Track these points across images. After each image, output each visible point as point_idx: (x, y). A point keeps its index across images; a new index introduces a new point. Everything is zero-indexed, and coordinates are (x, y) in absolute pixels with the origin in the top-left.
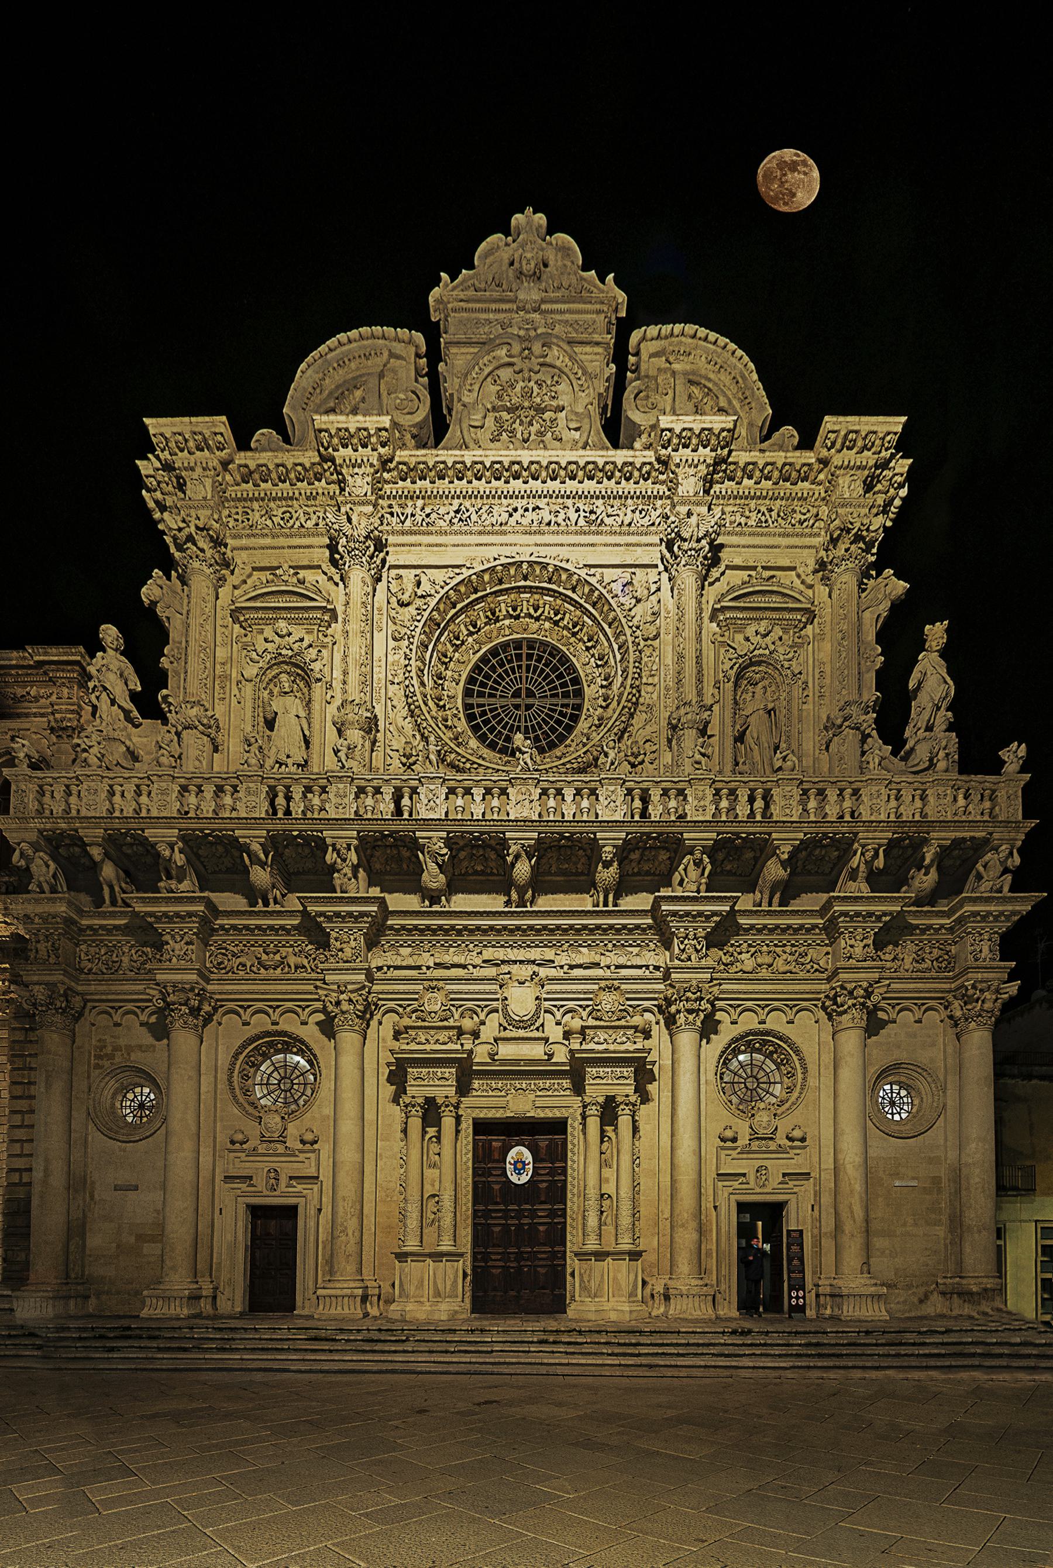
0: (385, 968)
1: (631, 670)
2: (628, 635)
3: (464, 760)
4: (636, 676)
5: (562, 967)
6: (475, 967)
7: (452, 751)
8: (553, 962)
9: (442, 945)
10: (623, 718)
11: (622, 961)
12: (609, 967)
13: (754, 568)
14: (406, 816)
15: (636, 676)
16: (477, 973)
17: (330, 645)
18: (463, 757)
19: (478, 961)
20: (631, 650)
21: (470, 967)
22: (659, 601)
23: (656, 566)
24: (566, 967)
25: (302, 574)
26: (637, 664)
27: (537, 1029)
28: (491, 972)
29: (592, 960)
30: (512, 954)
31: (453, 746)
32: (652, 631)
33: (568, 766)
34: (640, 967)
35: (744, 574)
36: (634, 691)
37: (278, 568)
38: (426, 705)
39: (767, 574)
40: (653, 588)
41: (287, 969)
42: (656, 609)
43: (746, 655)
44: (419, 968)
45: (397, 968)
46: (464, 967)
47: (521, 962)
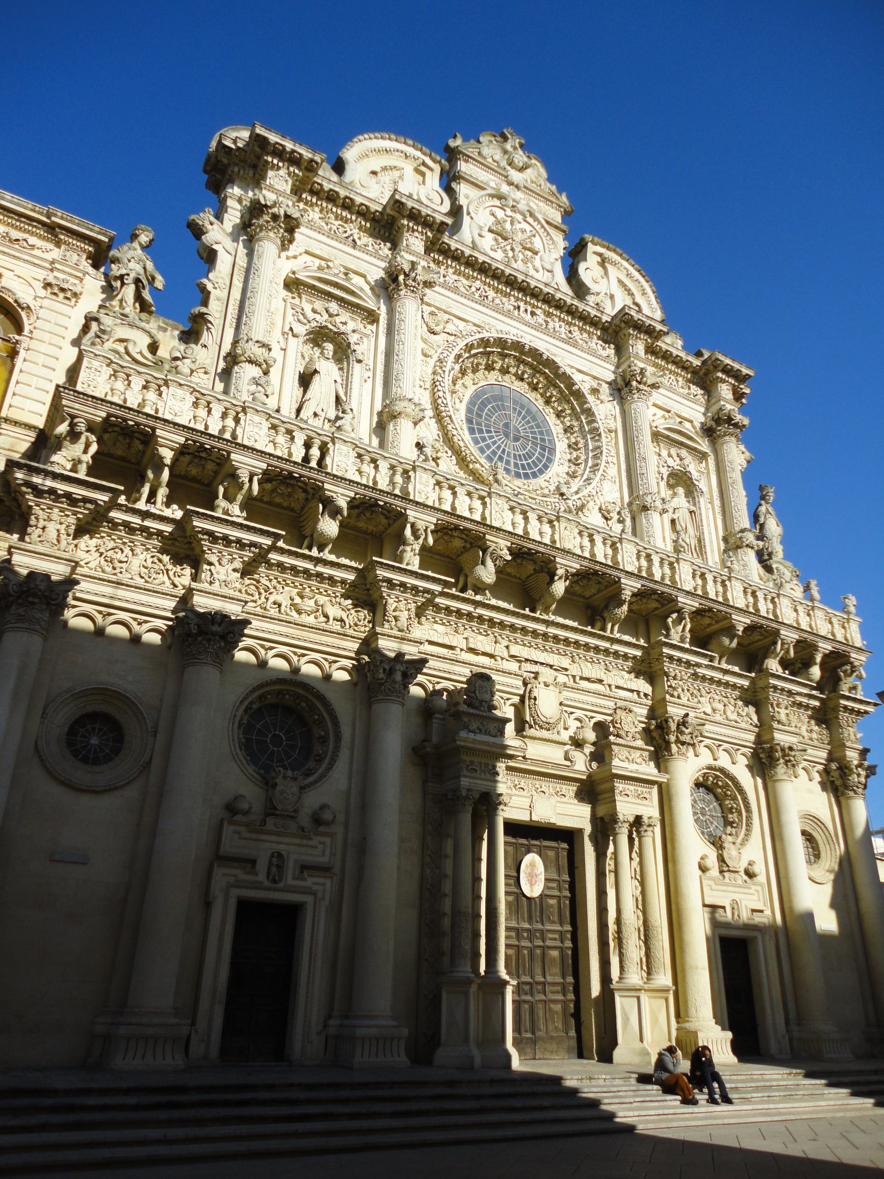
5: (574, 677)
6: (502, 659)
8: (566, 670)
11: (621, 683)
12: (610, 686)
13: (669, 412)
21: (499, 659)
25: (352, 275)
29: (599, 677)
34: (632, 691)
41: (325, 619)
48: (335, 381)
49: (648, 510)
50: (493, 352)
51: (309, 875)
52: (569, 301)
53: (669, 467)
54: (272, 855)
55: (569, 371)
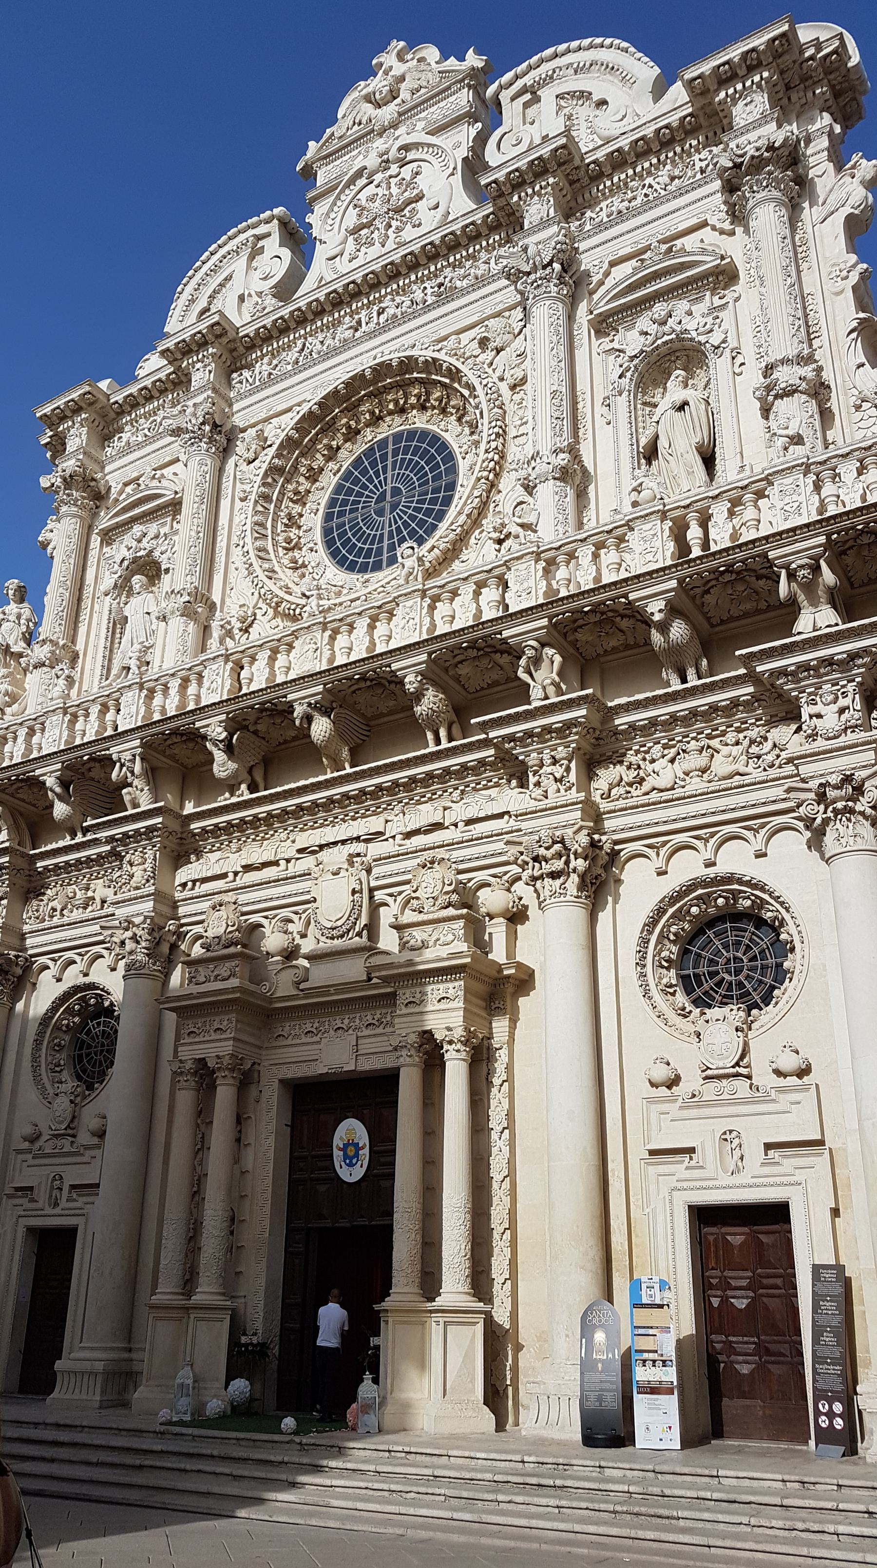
0: (190, 884)
3: (293, 607)
5: (393, 837)
6: (288, 861)
7: (282, 600)
9: (254, 840)
11: (471, 813)
12: (456, 825)
15: (493, 437)
16: (296, 868)
19: (292, 853)
24: (399, 837)
26: (493, 424)
27: (359, 934)
28: (307, 863)
30: (329, 834)
34: (500, 816)
35: (633, 263)
36: (490, 456)
37: (141, 476)
39: (664, 247)
43: (642, 351)
44: (224, 876)
45: (204, 880)
46: (276, 863)
47: (343, 842)
48: (148, 613)
51: (79, 1195)
52: (285, 312)
53: (632, 358)
54: (54, 1179)
55: (429, 354)
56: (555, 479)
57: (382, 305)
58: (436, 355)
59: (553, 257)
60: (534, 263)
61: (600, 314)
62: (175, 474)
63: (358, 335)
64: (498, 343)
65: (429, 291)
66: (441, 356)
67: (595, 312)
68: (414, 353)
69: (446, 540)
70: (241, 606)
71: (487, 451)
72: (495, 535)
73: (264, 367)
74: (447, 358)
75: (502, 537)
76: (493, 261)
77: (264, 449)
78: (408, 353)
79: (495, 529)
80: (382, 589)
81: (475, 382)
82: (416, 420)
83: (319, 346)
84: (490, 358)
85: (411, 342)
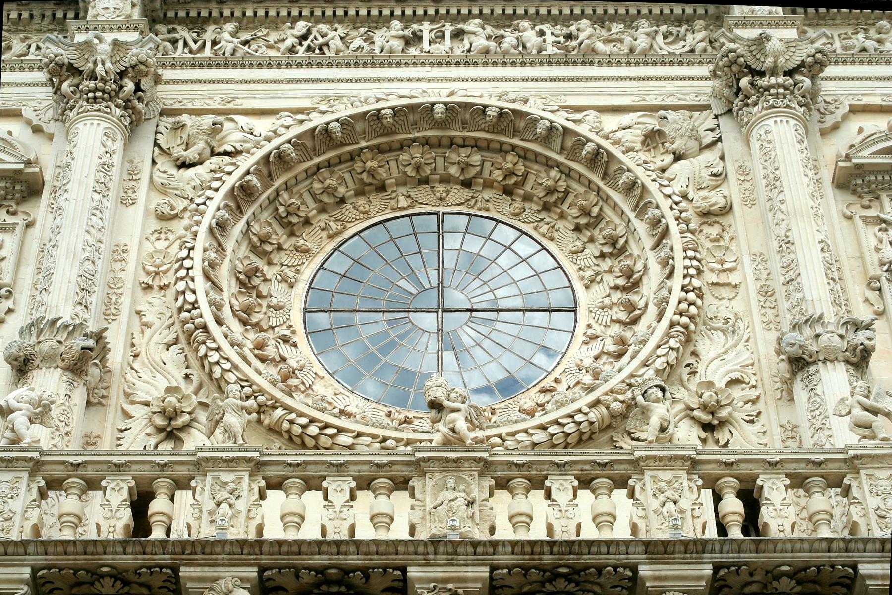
1: (680, 262)
2: (665, 204)
3: (304, 421)
4: (692, 271)
10: (673, 343)
14: (157, 533)
15: (692, 271)
17: (19, 229)
18: (301, 415)
20: (674, 228)
22: (722, 158)
23: (707, 107)
26: (690, 253)
31: (278, 395)
32: (716, 199)
33: (553, 429)
38: (219, 322)
40: (709, 138)
42: (718, 169)
49: (808, 364)
50: (361, 149)
55: (561, 119)
56: (848, 362)
57: (466, 27)
58: (570, 125)
59: (803, 64)
60: (775, 62)
61: (859, 166)
62: (10, 133)
63: (413, 51)
64: (678, 145)
65: (549, 38)
66: (583, 130)
67: (855, 161)
68: (533, 108)
69: (621, 398)
70: (170, 390)
71: (683, 289)
72: (706, 417)
73: (226, 36)
74: (592, 136)
75: (715, 422)
76: (659, 38)
77: (213, 153)
78: (517, 106)
79: (704, 407)
80: (498, 440)
81: (653, 187)
82: (490, 205)
83: (336, 43)
84: (665, 163)
85: (524, 93)
